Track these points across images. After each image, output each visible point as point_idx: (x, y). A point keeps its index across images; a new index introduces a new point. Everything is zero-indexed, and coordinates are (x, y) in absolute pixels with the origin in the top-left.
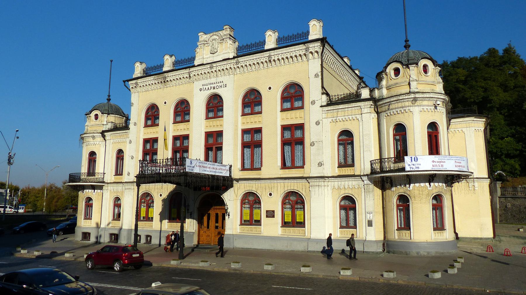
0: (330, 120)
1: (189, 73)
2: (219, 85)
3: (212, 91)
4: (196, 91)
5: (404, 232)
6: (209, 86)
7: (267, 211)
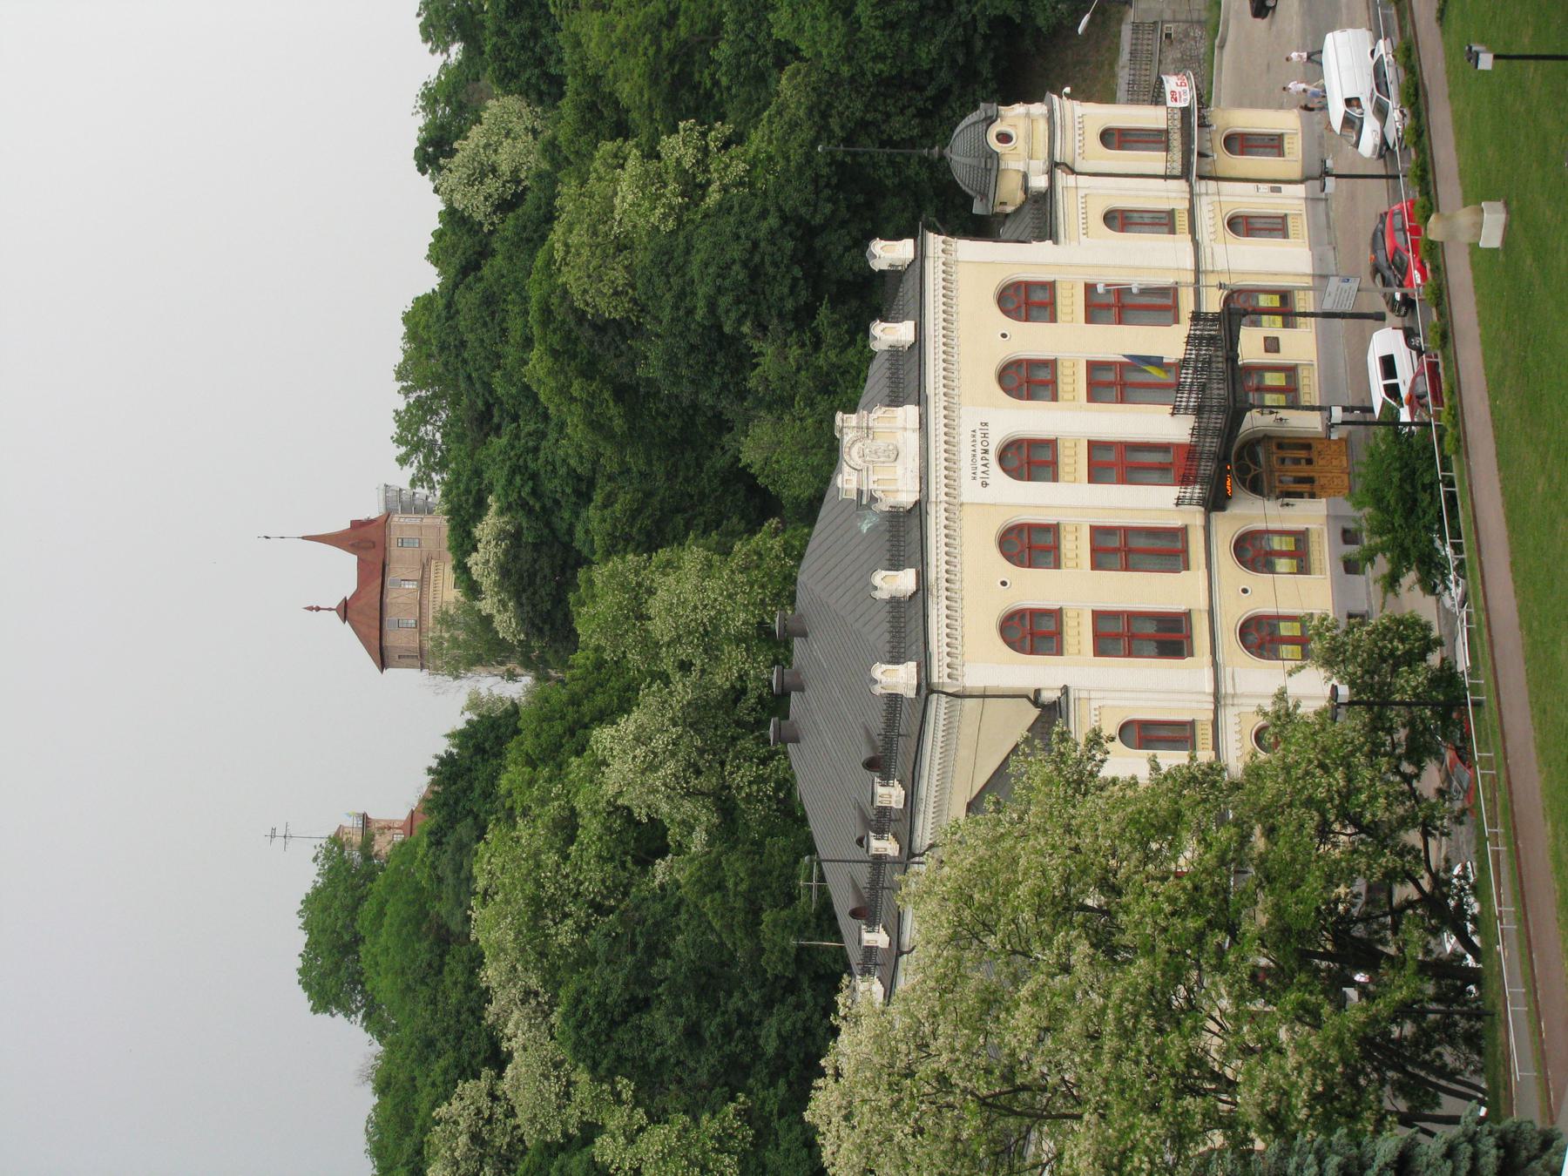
0: (1083, 238)
3: (992, 457)
4: (986, 496)
5: (1286, 146)
6: (980, 463)
7: (1267, 351)
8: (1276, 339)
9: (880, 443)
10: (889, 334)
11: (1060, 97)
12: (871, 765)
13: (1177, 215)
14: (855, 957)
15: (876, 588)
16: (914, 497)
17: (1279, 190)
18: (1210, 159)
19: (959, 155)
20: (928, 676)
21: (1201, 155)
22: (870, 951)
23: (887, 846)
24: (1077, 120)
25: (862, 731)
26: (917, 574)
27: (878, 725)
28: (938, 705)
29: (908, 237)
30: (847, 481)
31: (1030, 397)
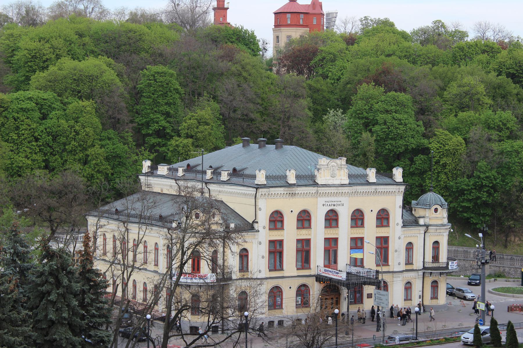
1: (317, 191)
2: (338, 203)
3: (332, 208)
4: (320, 205)
5: (434, 300)
6: (331, 203)
7: (368, 294)
8: (372, 297)
9: (337, 172)
10: (372, 174)
11: (450, 228)
12: (235, 170)
13: (411, 265)
14: (175, 166)
15: (290, 171)
16: (320, 183)
17: (420, 298)
18: (429, 275)
19: (431, 196)
20: (261, 188)
21: (431, 273)
22: (177, 170)
23: (209, 175)
24: (442, 234)
25: (245, 167)
26: (295, 184)
27: (247, 172)
28: (252, 191)
29: (403, 180)
30: (323, 161)
31: (352, 219)
